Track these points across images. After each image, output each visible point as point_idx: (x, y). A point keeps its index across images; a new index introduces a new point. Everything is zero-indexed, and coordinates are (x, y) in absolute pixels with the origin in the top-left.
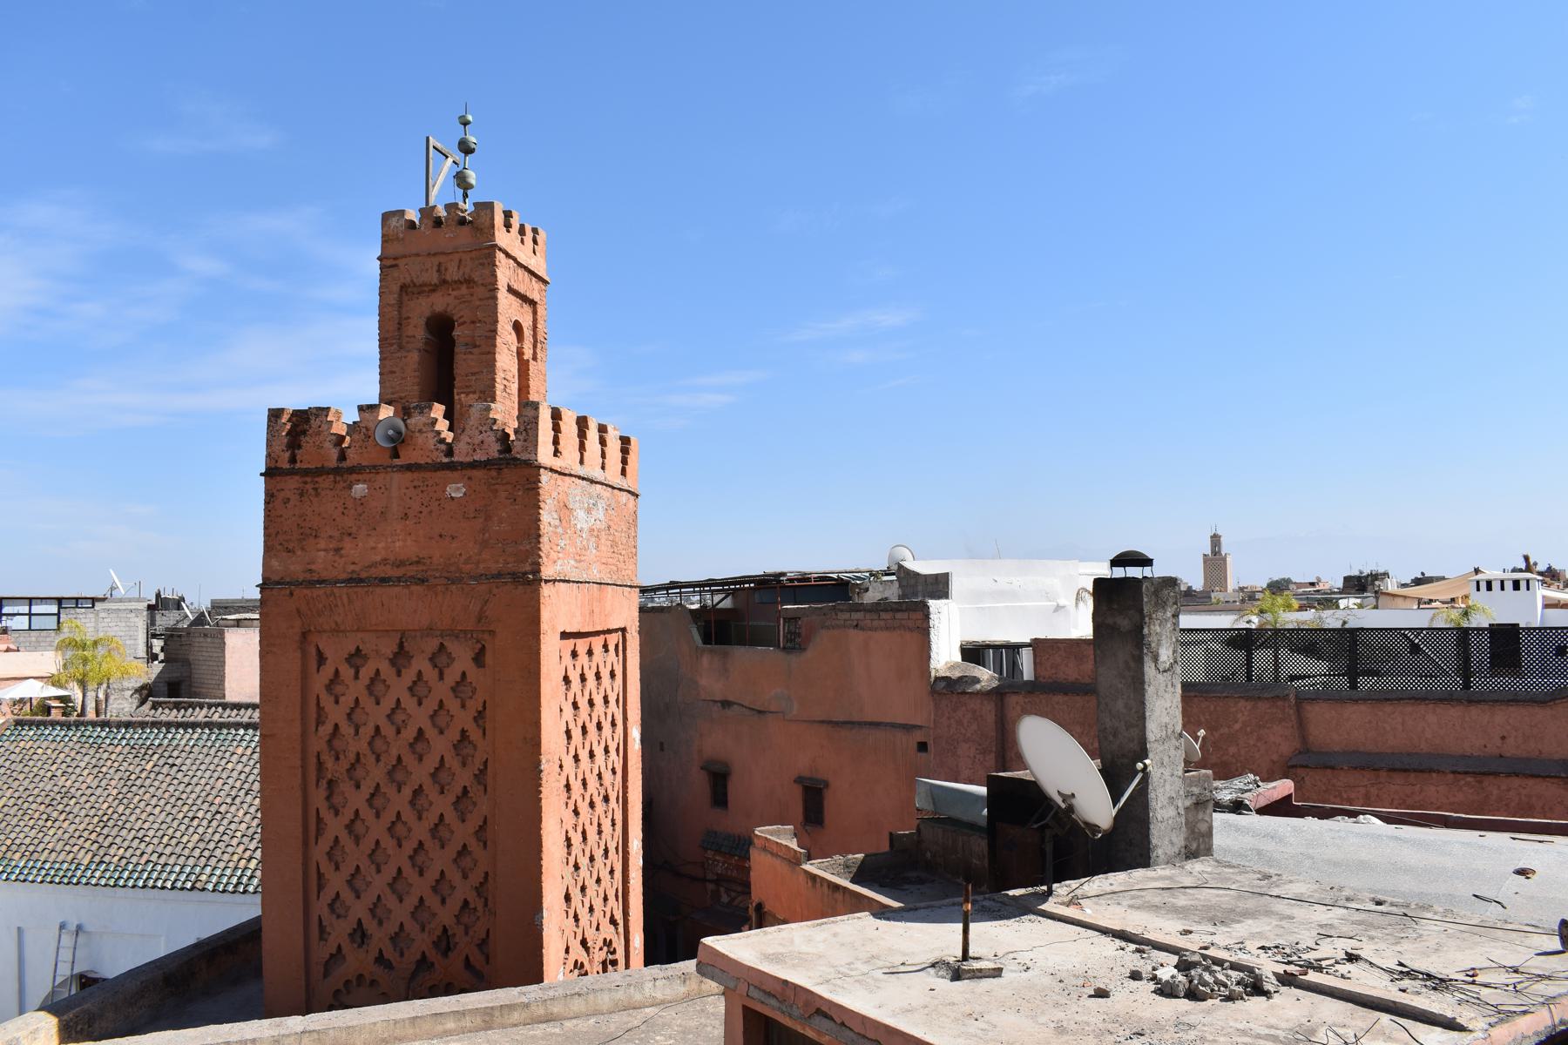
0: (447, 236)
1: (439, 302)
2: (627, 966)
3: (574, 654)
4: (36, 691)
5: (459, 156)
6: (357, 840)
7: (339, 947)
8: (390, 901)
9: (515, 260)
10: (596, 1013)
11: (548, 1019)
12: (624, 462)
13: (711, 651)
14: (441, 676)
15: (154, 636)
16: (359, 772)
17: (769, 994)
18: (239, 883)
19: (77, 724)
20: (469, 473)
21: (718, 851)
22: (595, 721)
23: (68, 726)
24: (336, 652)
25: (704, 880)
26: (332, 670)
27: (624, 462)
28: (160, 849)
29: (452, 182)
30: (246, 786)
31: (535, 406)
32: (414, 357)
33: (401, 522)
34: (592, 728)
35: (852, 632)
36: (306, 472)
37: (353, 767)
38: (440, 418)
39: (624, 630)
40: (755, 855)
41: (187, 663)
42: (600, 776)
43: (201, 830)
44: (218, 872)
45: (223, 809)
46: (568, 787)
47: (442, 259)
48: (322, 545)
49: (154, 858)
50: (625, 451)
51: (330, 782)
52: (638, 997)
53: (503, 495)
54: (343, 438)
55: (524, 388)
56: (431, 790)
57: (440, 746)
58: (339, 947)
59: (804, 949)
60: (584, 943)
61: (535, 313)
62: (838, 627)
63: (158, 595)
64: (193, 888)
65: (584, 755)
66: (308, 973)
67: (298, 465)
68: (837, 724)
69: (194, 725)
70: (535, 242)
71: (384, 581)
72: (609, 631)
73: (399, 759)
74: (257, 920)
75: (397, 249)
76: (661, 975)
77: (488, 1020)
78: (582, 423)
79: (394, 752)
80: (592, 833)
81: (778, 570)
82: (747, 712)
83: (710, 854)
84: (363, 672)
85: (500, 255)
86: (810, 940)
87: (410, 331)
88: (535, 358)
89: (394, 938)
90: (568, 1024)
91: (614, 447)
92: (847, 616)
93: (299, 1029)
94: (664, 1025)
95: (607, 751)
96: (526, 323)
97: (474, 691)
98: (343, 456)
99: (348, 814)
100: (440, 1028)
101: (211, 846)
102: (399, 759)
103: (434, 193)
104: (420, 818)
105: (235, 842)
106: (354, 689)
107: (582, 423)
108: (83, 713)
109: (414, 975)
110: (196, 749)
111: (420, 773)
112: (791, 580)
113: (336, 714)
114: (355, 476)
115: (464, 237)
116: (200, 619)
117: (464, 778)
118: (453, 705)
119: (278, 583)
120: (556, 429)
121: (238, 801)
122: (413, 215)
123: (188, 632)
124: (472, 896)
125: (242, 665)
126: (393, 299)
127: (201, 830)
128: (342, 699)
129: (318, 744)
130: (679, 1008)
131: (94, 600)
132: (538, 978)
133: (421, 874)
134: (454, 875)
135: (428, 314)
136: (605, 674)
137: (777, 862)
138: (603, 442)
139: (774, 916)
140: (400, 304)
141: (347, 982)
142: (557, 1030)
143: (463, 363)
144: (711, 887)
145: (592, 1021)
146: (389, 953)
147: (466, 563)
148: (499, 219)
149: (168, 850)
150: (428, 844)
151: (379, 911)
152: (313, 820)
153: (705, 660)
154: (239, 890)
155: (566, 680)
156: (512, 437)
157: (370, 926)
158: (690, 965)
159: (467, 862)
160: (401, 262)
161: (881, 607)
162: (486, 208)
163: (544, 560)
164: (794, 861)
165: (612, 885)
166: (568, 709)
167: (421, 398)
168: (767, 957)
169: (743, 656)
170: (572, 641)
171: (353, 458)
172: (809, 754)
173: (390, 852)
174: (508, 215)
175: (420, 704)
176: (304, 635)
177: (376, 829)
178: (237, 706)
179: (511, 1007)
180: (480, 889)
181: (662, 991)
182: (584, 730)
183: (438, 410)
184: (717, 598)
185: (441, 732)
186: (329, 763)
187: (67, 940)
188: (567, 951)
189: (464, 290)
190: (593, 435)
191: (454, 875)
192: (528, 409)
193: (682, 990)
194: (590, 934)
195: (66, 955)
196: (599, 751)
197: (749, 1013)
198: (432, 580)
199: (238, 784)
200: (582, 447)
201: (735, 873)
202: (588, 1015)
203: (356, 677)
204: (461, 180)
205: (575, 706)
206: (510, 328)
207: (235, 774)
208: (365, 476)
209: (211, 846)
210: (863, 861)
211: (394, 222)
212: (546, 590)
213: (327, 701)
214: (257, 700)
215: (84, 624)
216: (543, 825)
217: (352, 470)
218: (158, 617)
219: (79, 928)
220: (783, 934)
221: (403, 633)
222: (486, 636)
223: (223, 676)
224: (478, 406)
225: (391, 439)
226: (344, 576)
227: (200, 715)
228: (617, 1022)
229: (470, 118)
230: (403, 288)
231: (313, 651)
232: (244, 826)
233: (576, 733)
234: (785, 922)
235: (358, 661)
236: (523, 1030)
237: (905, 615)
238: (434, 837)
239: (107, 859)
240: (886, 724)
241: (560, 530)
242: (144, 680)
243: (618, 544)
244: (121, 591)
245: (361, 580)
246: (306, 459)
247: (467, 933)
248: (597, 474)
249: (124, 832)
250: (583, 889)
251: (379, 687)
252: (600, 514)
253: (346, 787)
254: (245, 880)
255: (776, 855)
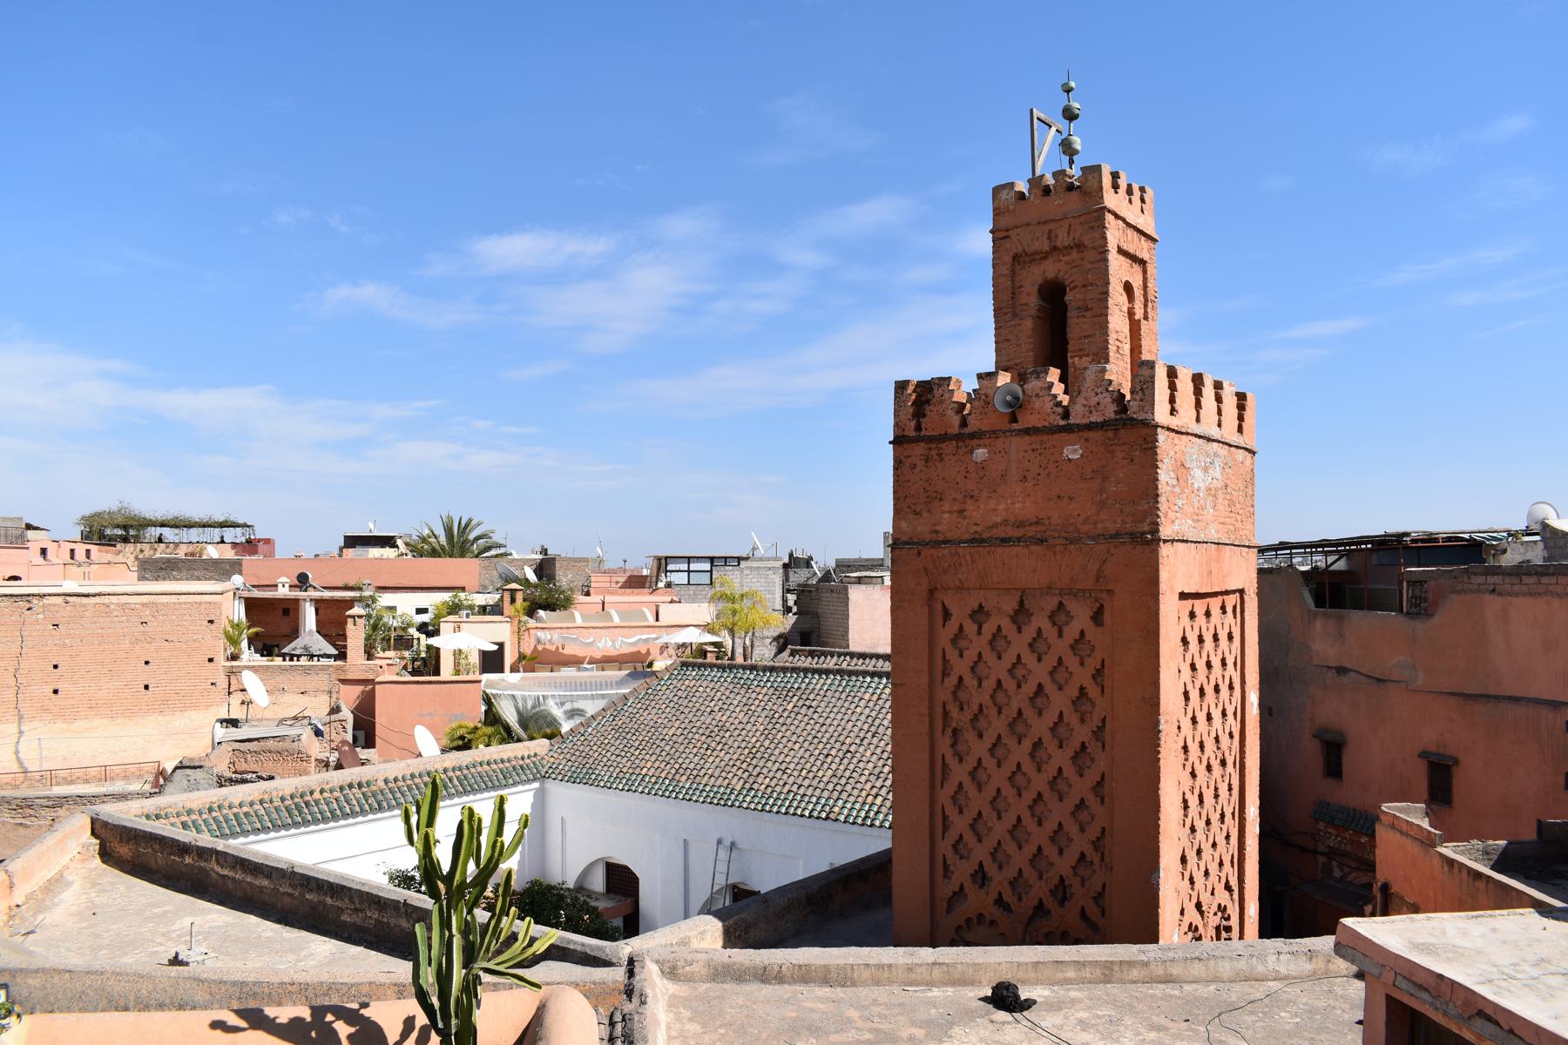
0: (1057, 203)
1: (1050, 269)
2: (1241, 937)
3: (1192, 615)
4: (694, 637)
5: (1062, 124)
6: (980, 787)
7: (962, 886)
8: (1010, 847)
9: (1124, 220)
10: (1216, 980)
11: (1168, 980)
12: (1241, 418)
13: (1325, 615)
14: (1060, 634)
15: (789, 591)
16: (982, 723)
17: (1420, 987)
18: (866, 817)
19: (731, 667)
20: (1086, 434)
21: (1331, 823)
22: (1213, 683)
23: (723, 668)
24: (961, 609)
25: (1315, 852)
26: (957, 626)
27: (1241, 418)
28: (799, 781)
29: (1058, 149)
30: (873, 729)
31: (1151, 365)
32: (1028, 324)
33: (1027, 483)
34: (1209, 690)
35: (1488, 597)
36: (931, 439)
37: (976, 718)
38: (1056, 382)
39: (1242, 592)
40: (1381, 832)
41: (817, 616)
42: (1217, 739)
43: (834, 766)
44: (849, 805)
45: (853, 749)
46: (1185, 748)
47: (1052, 226)
48: (946, 507)
49: (794, 788)
50: (1241, 407)
51: (955, 731)
52: (1260, 969)
53: (1120, 455)
54: (963, 405)
55: (1136, 348)
56: (1050, 744)
57: (1059, 701)
58: (962, 886)
59: (1459, 942)
60: (1199, 906)
61: (1145, 272)
62: (1472, 591)
63: (791, 555)
64: (827, 818)
65: (1202, 717)
66: (932, 907)
67: (923, 433)
68: (1469, 696)
69: (827, 672)
70: (1143, 200)
71: (1004, 540)
72: (1227, 593)
73: (1020, 712)
74: (887, 853)
75: (1006, 221)
76: (1285, 949)
77: (1108, 973)
78: (1198, 380)
79: (1015, 705)
80: (1209, 796)
81: (1401, 530)
82: (1365, 680)
83: (1322, 825)
84: (985, 627)
85: (1109, 217)
86: (1464, 934)
87: (1023, 299)
88: (1146, 318)
89: (1013, 883)
90: (1187, 987)
91: (1230, 403)
92: (1481, 579)
93: (931, 960)
94: (1289, 1001)
95: (1224, 714)
96: (1137, 283)
97: (1093, 649)
98: (964, 423)
99: (971, 763)
100: (1060, 976)
101: (843, 781)
102: (1020, 712)
103: (1040, 163)
104: (1039, 770)
105: (863, 779)
106: (978, 644)
107: (1198, 380)
108: (732, 658)
109: (1031, 919)
110: (829, 694)
111: (1040, 727)
112: (1413, 541)
113: (960, 667)
114: (976, 441)
115: (1073, 202)
116: (827, 577)
117: (1082, 733)
118: (1071, 662)
119: (907, 543)
120: (1172, 387)
121: (865, 742)
122: (1022, 186)
123: (817, 587)
124: (1088, 850)
125: (870, 619)
126: (1005, 270)
127: (834, 766)
128: (966, 653)
129: (944, 694)
130: (1305, 986)
131: (739, 559)
132: (1153, 937)
133: (1040, 824)
134: (1072, 828)
135: (1040, 280)
136: (1223, 636)
137: (1409, 841)
138: (1219, 399)
139: (1402, 898)
140: (1013, 273)
141: (968, 920)
142: (1176, 993)
143: (1076, 327)
144: (1321, 859)
145: (1212, 987)
146: (1008, 896)
147: (1084, 523)
148: (1107, 181)
149: (806, 783)
150: (1047, 795)
151: (999, 856)
152: (939, 765)
153: (1318, 625)
154: (867, 823)
155: (1185, 641)
156: (1128, 397)
157: (991, 869)
158: (1326, 943)
159: (1084, 816)
160: (1012, 234)
161: (1522, 570)
162: (1093, 171)
163: (1162, 520)
164: (1429, 843)
165: (1228, 851)
166: (1186, 670)
167: (1036, 364)
168: (1416, 947)
169: (1360, 621)
170: (1190, 602)
171: (974, 424)
172: (1438, 729)
173: (1010, 800)
174: (1115, 176)
175: (1040, 660)
176: (931, 592)
177: (998, 778)
178: (863, 656)
179: (1131, 964)
180: (1097, 844)
181: (1287, 966)
182: (1202, 692)
183: (1054, 374)
184: (1331, 559)
185: (1060, 688)
186: (955, 713)
187: (723, 855)
188: (1182, 913)
189: (1074, 255)
190: (1208, 392)
191: (1072, 828)
192: (1142, 370)
193: (1307, 967)
194: (1205, 898)
195: (722, 867)
196: (1216, 714)
197: (1393, 1005)
198: (1051, 540)
199: (866, 727)
200: (1198, 405)
201: (1349, 848)
202: (1209, 981)
203: (979, 633)
204: (1067, 147)
205: (1193, 667)
206: (1121, 289)
207: (863, 718)
208: (986, 441)
209: (843, 781)
210: (1506, 849)
211: (1004, 195)
212: (1165, 550)
213: (952, 655)
214: (888, 650)
215: (733, 580)
216: (1162, 785)
217: (973, 436)
218: (791, 574)
219: (733, 845)
220: (1432, 923)
221: (1023, 591)
222: (1104, 595)
223: (847, 628)
224: (1093, 368)
225: (1009, 405)
226: (967, 537)
227: (831, 663)
228: (1237, 992)
229: (1073, 84)
230: (1016, 257)
231: (940, 607)
232: (871, 765)
233: (1194, 695)
234: (1415, 909)
235: (981, 617)
236: (1143, 988)
237: (1553, 580)
238: (1052, 789)
239: (755, 786)
240: (1529, 700)
241: (1177, 490)
242: (781, 630)
243: (1234, 505)
244: (761, 552)
245: (983, 541)
246: (931, 426)
247: (1083, 885)
248: (1214, 432)
249: (769, 764)
250: (1199, 852)
251: (1001, 643)
252: (1216, 472)
253: (969, 736)
254: (872, 814)
255: (1406, 835)
